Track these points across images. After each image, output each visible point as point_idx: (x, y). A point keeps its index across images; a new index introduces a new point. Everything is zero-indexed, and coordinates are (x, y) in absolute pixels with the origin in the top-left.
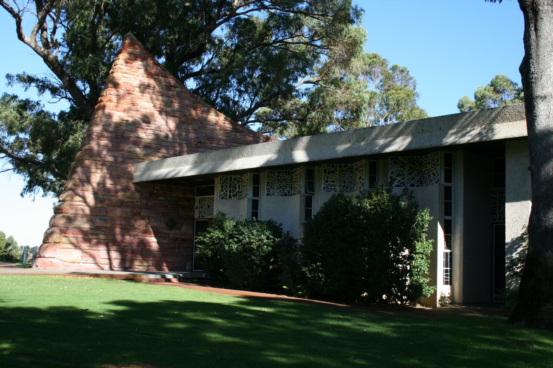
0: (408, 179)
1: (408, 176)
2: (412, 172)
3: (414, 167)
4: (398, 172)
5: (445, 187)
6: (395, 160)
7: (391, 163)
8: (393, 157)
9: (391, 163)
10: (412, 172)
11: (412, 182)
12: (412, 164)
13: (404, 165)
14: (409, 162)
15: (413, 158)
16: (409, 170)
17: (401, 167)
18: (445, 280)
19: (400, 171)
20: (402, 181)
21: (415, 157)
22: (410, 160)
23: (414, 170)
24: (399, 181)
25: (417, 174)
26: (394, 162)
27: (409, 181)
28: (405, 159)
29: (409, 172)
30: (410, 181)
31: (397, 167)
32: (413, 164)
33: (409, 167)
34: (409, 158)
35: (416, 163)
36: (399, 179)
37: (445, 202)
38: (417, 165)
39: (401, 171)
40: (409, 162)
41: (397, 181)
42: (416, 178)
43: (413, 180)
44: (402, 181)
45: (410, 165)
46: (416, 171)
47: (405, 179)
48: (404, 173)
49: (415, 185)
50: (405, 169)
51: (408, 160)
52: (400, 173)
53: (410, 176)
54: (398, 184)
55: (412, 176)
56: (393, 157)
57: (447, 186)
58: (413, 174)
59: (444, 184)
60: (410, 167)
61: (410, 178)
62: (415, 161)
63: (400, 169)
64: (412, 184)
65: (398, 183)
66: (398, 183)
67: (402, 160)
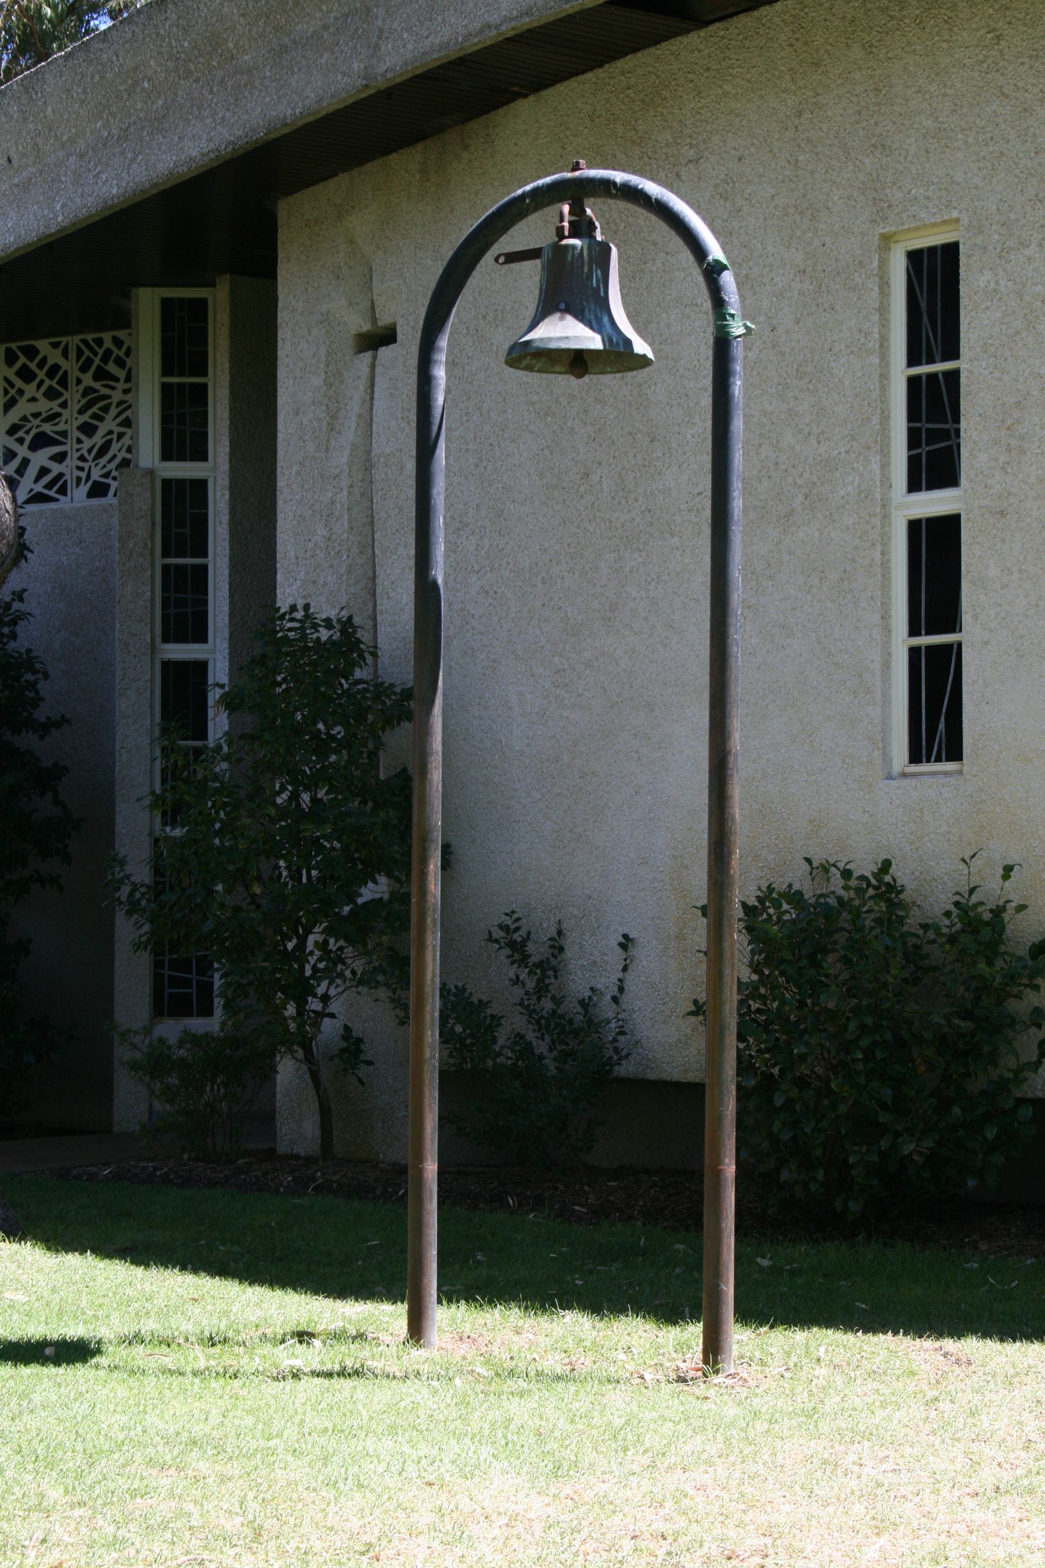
0: (82, 458)
1: (79, 441)
2: (95, 416)
3: (104, 391)
4: (37, 422)
5: (167, 483)
6: (22, 360)
7: (6, 379)
8: (13, 346)
9: (6, 379)
10: (95, 416)
11: (96, 475)
12: (96, 377)
13: (63, 382)
14: (84, 369)
15: (99, 342)
16: (81, 412)
17: (51, 394)
18: (167, 991)
19: (43, 421)
20: (56, 468)
21: (107, 337)
22: (87, 352)
23: (106, 409)
24: (43, 471)
25: (117, 430)
26: (18, 374)
27: (81, 469)
28: (65, 354)
29: (85, 418)
30: (86, 465)
31: (33, 399)
32: (101, 375)
33: (84, 395)
34: (85, 342)
35: (112, 368)
36: (41, 458)
37: (166, 568)
38: (117, 380)
39: (53, 417)
40: (84, 369)
41: (32, 471)
42: (114, 447)
43: (103, 461)
44: (56, 468)
45: (88, 380)
46: (113, 411)
47: (67, 462)
48: (61, 427)
49: (108, 486)
50: (64, 405)
51: (80, 353)
52: (47, 428)
53: (88, 443)
54: (39, 488)
55: (98, 439)
56: (13, 346)
57: (181, 482)
58: (103, 428)
59: (151, 472)
60: (88, 391)
61: (90, 451)
62: (105, 359)
63: (44, 406)
64: (95, 482)
65: (36, 481)
66: (36, 481)
67: (55, 357)
